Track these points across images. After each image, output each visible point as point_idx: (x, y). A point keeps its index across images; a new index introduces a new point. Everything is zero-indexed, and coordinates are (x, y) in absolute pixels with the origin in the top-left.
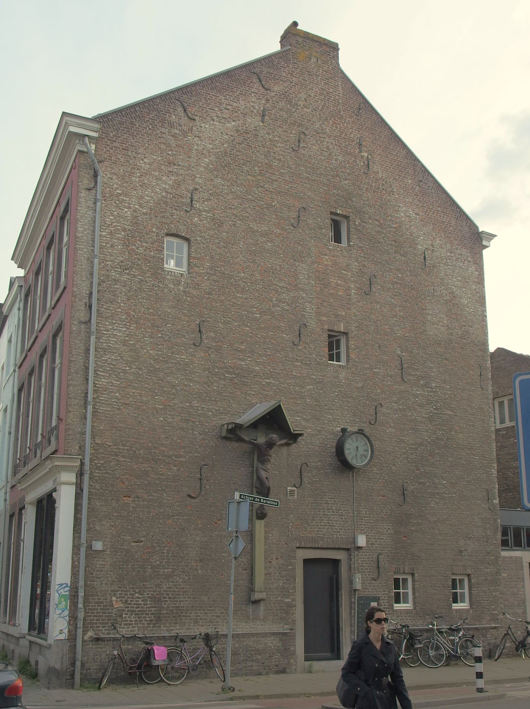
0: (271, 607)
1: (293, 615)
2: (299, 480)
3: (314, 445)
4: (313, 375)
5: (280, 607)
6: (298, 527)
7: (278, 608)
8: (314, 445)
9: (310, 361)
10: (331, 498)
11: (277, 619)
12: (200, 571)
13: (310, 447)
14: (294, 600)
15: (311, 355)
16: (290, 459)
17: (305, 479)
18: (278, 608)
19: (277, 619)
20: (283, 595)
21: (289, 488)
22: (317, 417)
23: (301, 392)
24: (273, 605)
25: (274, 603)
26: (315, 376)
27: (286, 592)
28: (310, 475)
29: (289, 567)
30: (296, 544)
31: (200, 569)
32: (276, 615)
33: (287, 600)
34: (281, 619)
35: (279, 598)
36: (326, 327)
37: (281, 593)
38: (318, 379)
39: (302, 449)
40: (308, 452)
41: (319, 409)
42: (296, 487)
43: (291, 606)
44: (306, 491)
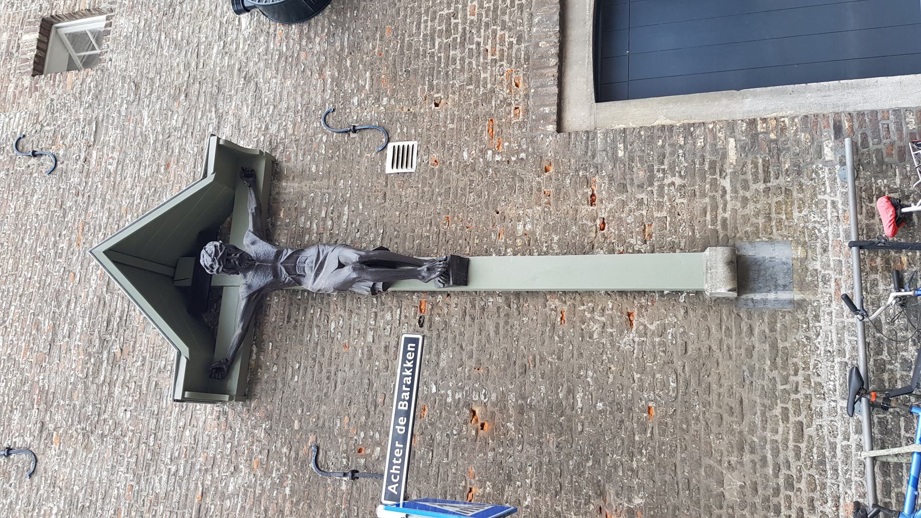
0: (757, 215)
1: (783, 129)
2: (368, 135)
3: (281, 93)
4: (119, 112)
5: (756, 180)
6: (496, 129)
7: (761, 186)
8: (281, 93)
9: (90, 124)
10: (419, 24)
11: (801, 189)
12: (638, 501)
13: (284, 105)
14: (731, 126)
15: (78, 120)
16: (314, 169)
17: (369, 115)
18: (761, 186)
19: (801, 189)
21: (389, 170)
22: (215, 90)
23: (155, 142)
24: (751, 208)
25: (745, 201)
26: (122, 103)
27: (702, 163)
28: (355, 100)
29: (621, 154)
31: (630, 501)
32: (788, 192)
33: (732, 156)
34: (799, 173)
35: (726, 183)
36: (27, 81)
37: (709, 177)
38: (129, 95)
39: (290, 131)
40: (296, 112)
41: (197, 85)
42: (385, 147)
43: (752, 133)
44: (397, 109)
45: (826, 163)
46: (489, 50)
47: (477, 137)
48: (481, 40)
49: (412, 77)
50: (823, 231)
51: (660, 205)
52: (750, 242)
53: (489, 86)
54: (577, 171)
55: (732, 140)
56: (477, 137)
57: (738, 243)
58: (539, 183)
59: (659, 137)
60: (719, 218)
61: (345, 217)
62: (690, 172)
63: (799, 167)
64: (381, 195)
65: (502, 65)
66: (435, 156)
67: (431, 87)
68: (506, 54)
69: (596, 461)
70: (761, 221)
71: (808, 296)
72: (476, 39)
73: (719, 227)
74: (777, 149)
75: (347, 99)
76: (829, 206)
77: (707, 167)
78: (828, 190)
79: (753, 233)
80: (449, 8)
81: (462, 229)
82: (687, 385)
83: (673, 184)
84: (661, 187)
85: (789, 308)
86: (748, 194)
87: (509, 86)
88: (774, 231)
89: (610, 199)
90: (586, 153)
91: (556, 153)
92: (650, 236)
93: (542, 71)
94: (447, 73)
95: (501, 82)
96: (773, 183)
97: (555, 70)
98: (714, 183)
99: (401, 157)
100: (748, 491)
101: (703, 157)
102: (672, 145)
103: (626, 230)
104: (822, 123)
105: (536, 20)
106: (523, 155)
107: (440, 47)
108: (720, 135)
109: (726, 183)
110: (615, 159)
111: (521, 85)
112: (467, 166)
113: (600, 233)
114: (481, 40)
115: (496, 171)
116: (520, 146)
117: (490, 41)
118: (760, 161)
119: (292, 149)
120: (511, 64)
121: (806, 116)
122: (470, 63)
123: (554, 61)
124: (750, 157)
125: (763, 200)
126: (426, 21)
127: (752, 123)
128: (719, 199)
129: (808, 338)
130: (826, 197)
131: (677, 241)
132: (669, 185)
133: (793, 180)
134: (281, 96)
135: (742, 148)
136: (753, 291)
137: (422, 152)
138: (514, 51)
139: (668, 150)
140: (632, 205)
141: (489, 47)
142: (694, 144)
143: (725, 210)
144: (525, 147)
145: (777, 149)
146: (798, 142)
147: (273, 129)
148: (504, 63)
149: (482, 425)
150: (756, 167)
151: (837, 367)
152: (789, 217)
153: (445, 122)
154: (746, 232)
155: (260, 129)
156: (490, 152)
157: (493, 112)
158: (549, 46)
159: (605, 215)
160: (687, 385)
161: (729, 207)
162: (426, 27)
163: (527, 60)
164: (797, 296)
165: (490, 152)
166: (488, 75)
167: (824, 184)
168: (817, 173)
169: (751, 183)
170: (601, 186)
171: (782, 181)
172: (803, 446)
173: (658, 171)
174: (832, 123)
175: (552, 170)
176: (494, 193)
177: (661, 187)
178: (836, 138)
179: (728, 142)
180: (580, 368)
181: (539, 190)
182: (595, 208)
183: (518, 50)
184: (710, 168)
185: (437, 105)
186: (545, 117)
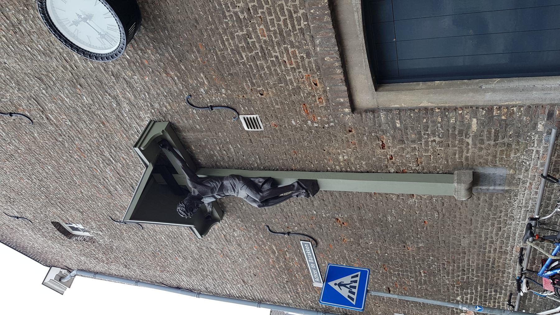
5: (489, 139)
7: (492, 143)
18: (492, 143)
20: (461, 132)
24: (484, 152)
25: (481, 149)
30: (345, 114)
32: (509, 145)
35: (470, 141)
45: (537, 133)
46: (287, 61)
47: (298, 113)
48: (278, 54)
49: (235, 77)
50: (528, 163)
51: (426, 151)
52: (482, 167)
53: (295, 84)
54: (370, 133)
55: (475, 120)
56: (298, 113)
57: (474, 167)
58: (347, 138)
59: (424, 118)
60: (464, 156)
61: (232, 150)
62: (446, 135)
63: (519, 133)
64: (248, 141)
65: (300, 72)
66: (274, 122)
67: (253, 84)
68: (300, 64)
69: (400, 235)
70: (490, 158)
71: (513, 188)
72: (274, 54)
73: (463, 160)
74: (506, 125)
75: (196, 90)
76: (534, 152)
77: (457, 133)
78: (536, 145)
79: (484, 163)
80: (242, 31)
81: (305, 157)
82: (444, 215)
83: (434, 141)
84: (427, 143)
85: (502, 192)
86: (483, 146)
87: (310, 85)
88: (497, 162)
89: (394, 146)
90: (375, 125)
91: (355, 123)
92: (421, 163)
93: (332, 76)
94: (260, 76)
95: (303, 83)
96: (500, 141)
97: (342, 76)
98: (461, 141)
99: (251, 123)
100: (472, 245)
101: (454, 128)
102: (433, 122)
103: (406, 161)
104: (540, 111)
105: (318, 42)
106: (332, 124)
107: (248, 59)
108: (466, 116)
109: (470, 141)
110: (395, 128)
111: (318, 84)
112: (297, 128)
113: (390, 161)
114: (278, 54)
115: (317, 132)
116: (328, 119)
117: (285, 55)
118: (493, 130)
119: (177, 117)
120: (307, 71)
121: (530, 107)
122: (275, 70)
123: (339, 71)
124: (486, 128)
125: (492, 149)
126: (228, 40)
127: (490, 109)
128: (464, 147)
129: (509, 202)
130: (533, 148)
131: (438, 166)
132: (432, 141)
133: (513, 140)
134: (147, 87)
135: (481, 124)
136: (482, 185)
137: (263, 120)
138: (306, 63)
139: (430, 124)
140: (409, 150)
141: (285, 59)
142: (448, 121)
143: (467, 152)
144: (332, 120)
145: (506, 125)
146: (521, 121)
147: (156, 106)
148: (301, 70)
149: (343, 223)
150: (490, 133)
151: (522, 212)
152: (508, 156)
153: (272, 105)
154: (480, 162)
155: (147, 105)
156: (309, 122)
157: (303, 100)
158: (332, 59)
159: (393, 154)
160: (444, 215)
161: (470, 151)
162: (230, 44)
163: (318, 69)
164: (507, 188)
165: (309, 122)
166: (292, 77)
167: (534, 142)
168: (530, 137)
169: (485, 141)
170: (387, 140)
171: (506, 140)
172: (500, 233)
173: (424, 134)
174: (547, 112)
175: (354, 132)
176: (320, 142)
177: (427, 143)
178: (548, 119)
179: (472, 121)
180: (388, 209)
181: (348, 141)
182: (385, 150)
183: (310, 62)
184: (459, 134)
185: (262, 95)
186: (342, 104)
